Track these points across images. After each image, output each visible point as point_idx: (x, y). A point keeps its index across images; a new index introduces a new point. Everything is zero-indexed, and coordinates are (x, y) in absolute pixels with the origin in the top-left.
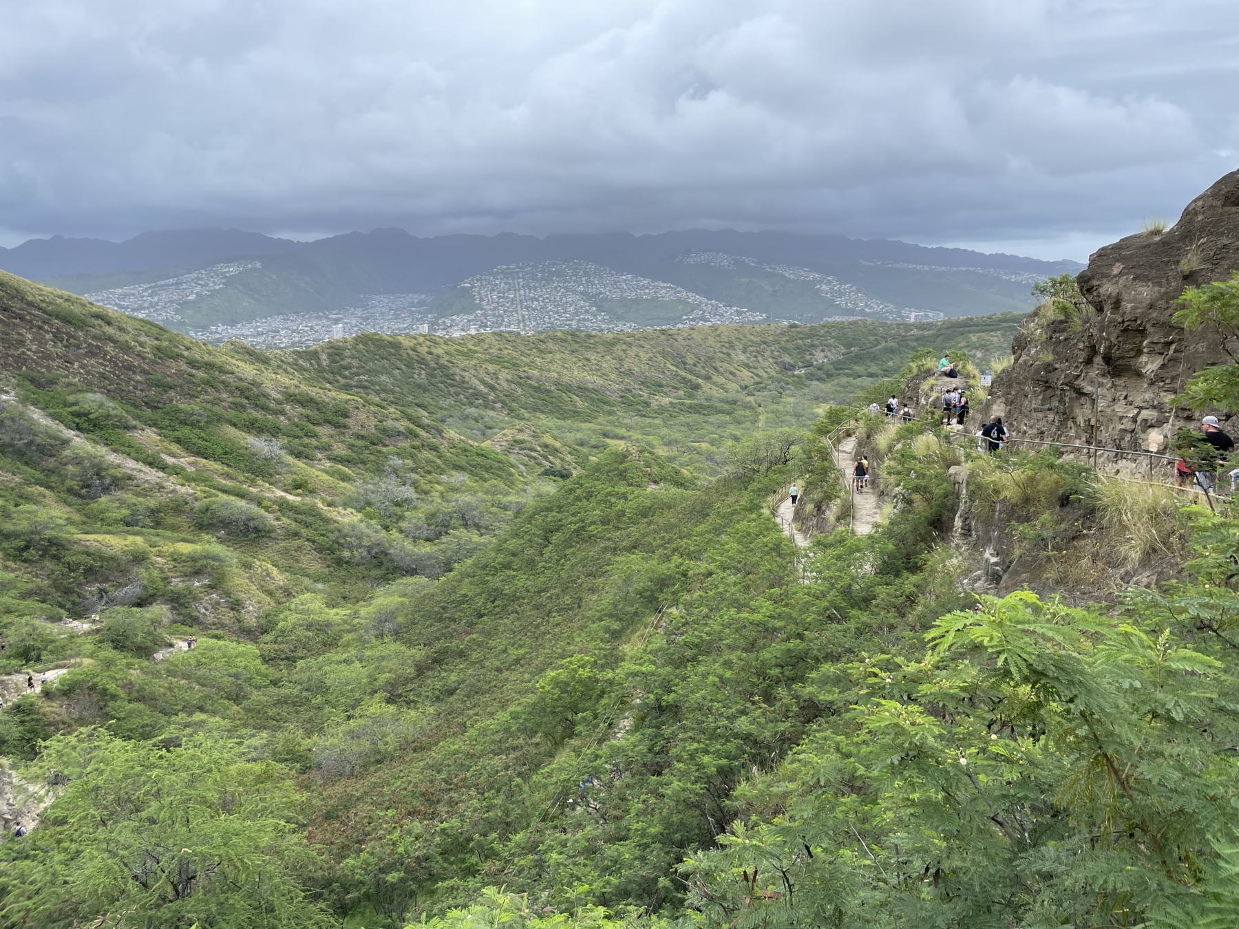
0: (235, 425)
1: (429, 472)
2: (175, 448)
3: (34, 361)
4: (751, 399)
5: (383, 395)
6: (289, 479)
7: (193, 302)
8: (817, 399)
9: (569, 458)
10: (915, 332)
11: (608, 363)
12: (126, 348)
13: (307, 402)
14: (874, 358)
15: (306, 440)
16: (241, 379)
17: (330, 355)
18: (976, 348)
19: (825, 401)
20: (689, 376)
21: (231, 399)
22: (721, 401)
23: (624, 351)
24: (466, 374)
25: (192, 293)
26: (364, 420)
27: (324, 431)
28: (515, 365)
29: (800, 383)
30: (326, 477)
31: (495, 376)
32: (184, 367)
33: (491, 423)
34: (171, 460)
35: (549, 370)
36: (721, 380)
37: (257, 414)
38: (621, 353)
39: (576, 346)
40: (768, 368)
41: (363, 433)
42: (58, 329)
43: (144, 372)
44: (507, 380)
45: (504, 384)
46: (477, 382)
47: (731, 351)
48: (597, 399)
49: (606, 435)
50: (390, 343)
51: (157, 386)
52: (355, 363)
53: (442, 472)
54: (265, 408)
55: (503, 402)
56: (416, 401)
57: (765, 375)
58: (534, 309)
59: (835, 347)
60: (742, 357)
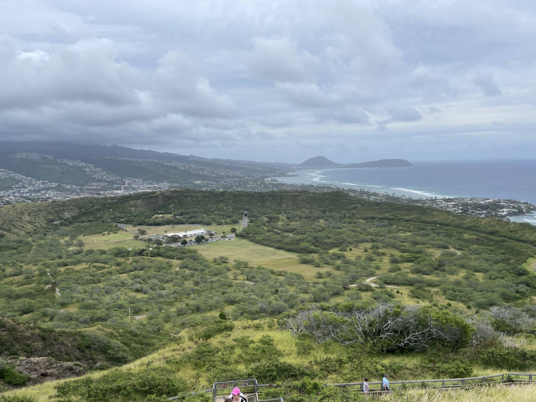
4: (30, 239)
8: (63, 235)
10: (109, 201)
14: (92, 213)
18: (132, 207)
19: (67, 235)
22: (14, 241)
29: (56, 228)
36: (16, 230)
40: (41, 222)
47: (22, 216)
57: (39, 226)
59: (74, 210)
60: (28, 218)
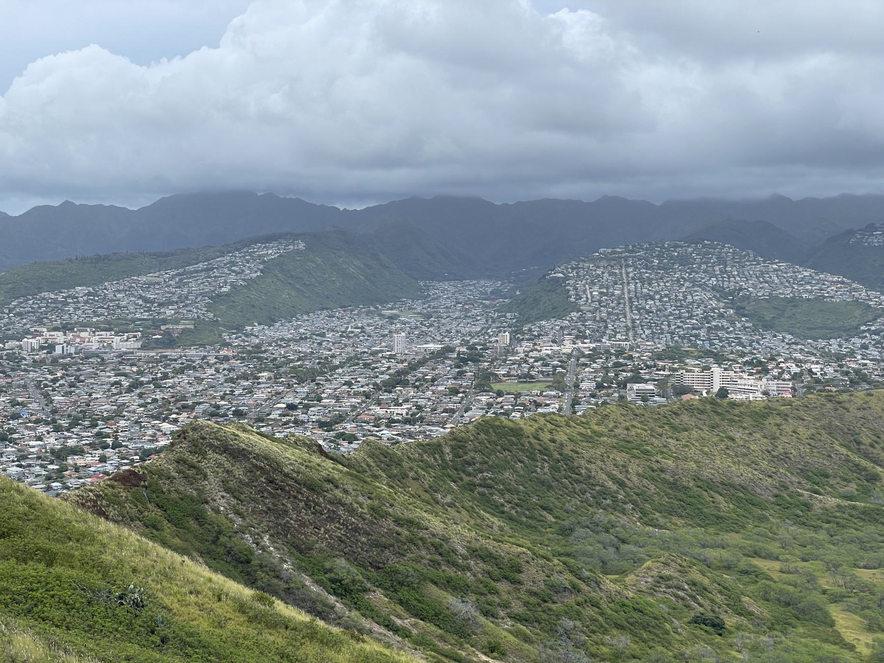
0: (436, 583)
1: (594, 632)
2: (399, 609)
3: (295, 529)
5: (507, 496)
6: (484, 640)
7: (227, 295)
9: (719, 598)
11: (758, 444)
12: (351, 511)
13: (485, 556)
15: (490, 598)
16: (434, 535)
17: (453, 448)
20: (864, 463)
21: (429, 557)
23: (778, 425)
24: (593, 466)
25: (225, 283)
26: (533, 576)
27: (503, 586)
28: (646, 452)
30: (512, 638)
31: (624, 468)
32: (392, 526)
33: (623, 535)
34: (399, 622)
35: (686, 459)
37: (451, 572)
38: (775, 429)
39: (717, 419)
41: (535, 589)
42: (307, 498)
43: (367, 534)
44: (638, 475)
45: (635, 479)
46: (604, 477)
48: (744, 497)
49: (756, 554)
50: (512, 430)
51: (377, 546)
52: (478, 457)
53: (605, 632)
54: (454, 564)
55: (634, 503)
56: (541, 503)
58: (648, 312)
